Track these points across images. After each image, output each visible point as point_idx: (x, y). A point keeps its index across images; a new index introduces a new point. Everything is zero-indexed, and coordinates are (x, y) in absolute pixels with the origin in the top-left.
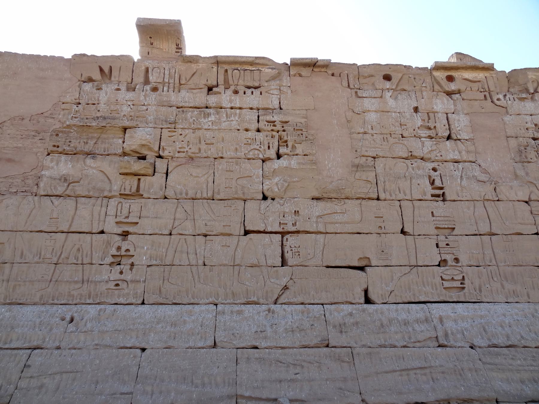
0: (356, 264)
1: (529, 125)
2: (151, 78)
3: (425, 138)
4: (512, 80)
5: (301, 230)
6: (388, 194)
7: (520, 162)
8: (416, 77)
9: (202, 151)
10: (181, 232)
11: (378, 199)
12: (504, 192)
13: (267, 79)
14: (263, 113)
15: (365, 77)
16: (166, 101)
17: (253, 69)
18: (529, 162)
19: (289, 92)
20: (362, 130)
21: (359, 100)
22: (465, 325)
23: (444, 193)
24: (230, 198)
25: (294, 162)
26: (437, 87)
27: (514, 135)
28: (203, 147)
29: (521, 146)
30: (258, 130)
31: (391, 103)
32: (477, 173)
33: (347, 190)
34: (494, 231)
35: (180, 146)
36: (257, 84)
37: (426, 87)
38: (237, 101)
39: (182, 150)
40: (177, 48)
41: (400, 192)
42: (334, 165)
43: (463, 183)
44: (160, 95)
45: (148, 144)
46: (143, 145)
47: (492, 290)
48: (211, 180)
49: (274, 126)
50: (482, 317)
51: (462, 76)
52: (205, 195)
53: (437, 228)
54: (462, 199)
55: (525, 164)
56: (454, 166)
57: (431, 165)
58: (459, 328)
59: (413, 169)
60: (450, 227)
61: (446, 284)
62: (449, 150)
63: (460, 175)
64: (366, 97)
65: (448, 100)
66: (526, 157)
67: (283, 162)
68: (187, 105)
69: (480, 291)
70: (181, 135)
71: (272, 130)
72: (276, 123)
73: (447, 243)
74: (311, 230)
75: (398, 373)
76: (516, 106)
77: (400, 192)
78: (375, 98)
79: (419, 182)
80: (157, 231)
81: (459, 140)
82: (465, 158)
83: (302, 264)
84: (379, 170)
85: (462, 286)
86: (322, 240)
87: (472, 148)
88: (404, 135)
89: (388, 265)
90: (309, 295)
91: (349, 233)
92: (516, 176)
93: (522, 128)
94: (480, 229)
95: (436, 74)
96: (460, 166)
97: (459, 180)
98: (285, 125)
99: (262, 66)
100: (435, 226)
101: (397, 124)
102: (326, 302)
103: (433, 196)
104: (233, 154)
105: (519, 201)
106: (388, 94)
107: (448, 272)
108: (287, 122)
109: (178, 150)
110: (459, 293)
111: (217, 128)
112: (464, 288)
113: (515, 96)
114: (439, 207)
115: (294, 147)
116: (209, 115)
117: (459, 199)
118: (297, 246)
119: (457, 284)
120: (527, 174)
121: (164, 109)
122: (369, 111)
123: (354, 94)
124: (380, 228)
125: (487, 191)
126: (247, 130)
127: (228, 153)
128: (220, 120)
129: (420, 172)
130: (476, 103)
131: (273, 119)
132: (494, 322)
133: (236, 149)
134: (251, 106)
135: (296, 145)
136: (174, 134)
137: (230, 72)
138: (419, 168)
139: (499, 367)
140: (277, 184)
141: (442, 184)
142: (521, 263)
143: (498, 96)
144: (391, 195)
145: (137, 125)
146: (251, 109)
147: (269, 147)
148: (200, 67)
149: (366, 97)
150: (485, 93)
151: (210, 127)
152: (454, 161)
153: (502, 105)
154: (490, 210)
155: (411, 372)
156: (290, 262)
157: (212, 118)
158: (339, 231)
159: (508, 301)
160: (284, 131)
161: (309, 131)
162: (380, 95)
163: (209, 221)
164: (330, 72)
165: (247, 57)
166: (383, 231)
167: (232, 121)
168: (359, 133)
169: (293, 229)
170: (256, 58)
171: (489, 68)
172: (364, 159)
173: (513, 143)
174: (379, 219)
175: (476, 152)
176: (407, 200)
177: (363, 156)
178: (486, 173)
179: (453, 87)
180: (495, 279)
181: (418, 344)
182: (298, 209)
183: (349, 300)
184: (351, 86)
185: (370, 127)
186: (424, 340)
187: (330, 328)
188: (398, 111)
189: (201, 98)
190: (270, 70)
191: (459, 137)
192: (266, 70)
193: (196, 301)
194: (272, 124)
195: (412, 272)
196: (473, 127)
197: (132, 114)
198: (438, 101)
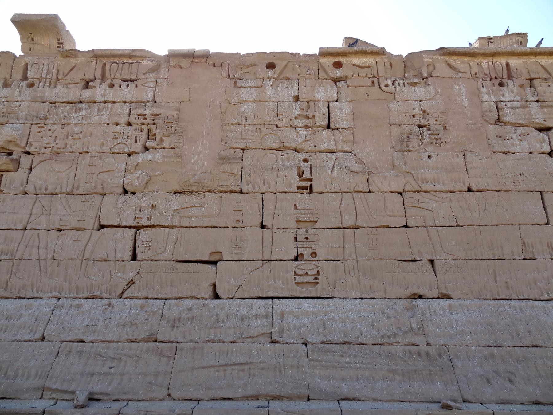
0: (206, 258)
1: (416, 112)
2: (29, 74)
3: (302, 128)
4: (408, 64)
5: (156, 224)
6: (251, 186)
7: (400, 151)
8: (302, 64)
9: (68, 146)
10: (35, 227)
11: (241, 192)
12: (377, 183)
13: (145, 71)
14: (136, 106)
15: (248, 67)
16: (40, 97)
17: (132, 62)
18: (410, 151)
19: (166, 84)
20: (235, 121)
21: (237, 90)
22: (307, 321)
23: (311, 185)
24: (89, 193)
25: (158, 156)
26: (322, 74)
27: (397, 122)
28: (70, 141)
29: (404, 134)
30: (130, 124)
31: (270, 92)
32: (351, 163)
33: (209, 183)
34: (359, 224)
35: (47, 142)
36: (134, 77)
37: (310, 74)
38: (111, 95)
39: (48, 145)
40: (59, 43)
41: (264, 185)
42: (200, 158)
43: (333, 174)
44: (35, 91)
45: (14, 140)
46: (9, 141)
47: (346, 285)
48: (72, 175)
49: (145, 119)
50: (326, 313)
51: (350, 61)
52: (64, 190)
53: (298, 221)
54: (329, 191)
55: (405, 153)
56: (327, 157)
57: (301, 156)
58: (298, 324)
59: (282, 161)
60: (312, 220)
61: (299, 279)
62: (325, 140)
63: (332, 165)
64: (246, 87)
65: (332, 88)
66: (407, 146)
67: (148, 156)
68: (60, 100)
69: (334, 286)
70: (50, 130)
71: (143, 124)
72: (146, 117)
73: (306, 236)
74: (166, 224)
75: (215, 369)
76: (405, 91)
77: (264, 185)
78: (254, 87)
79: (286, 174)
80: (11, 226)
81: (338, 129)
82: (340, 148)
83: (152, 258)
84: (246, 162)
85: (315, 281)
86: (175, 234)
87: (351, 137)
88: (279, 125)
89: (240, 259)
90: (154, 290)
91: (205, 227)
92: (394, 166)
93: (408, 115)
94: (344, 222)
95: (323, 60)
96: (334, 156)
97: (330, 171)
98: (155, 118)
99: (142, 59)
100: (296, 219)
101: (274, 114)
102: (170, 297)
103: (298, 188)
104: (98, 149)
105: (391, 192)
106: (268, 83)
107: (302, 266)
108: (158, 115)
109: (45, 145)
110: (310, 289)
111: (86, 122)
112: (318, 283)
113: (406, 81)
114: (305, 200)
115: (162, 140)
116: (80, 109)
117: (326, 191)
118: (149, 240)
119: (311, 279)
120: (406, 163)
121: (37, 104)
122: (246, 101)
123: (232, 84)
124: (238, 222)
125: (360, 182)
126: (117, 124)
127: (94, 148)
128: (91, 114)
129: (288, 164)
130: (362, 90)
131: (145, 113)
132: (337, 318)
133: (103, 143)
134: (124, 100)
135: (164, 138)
136: (43, 129)
137: (108, 66)
138: (288, 159)
139: (324, 364)
140: (138, 178)
141: (311, 176)
142: (384, 258)
143: (386, 82)
144: (254, 188)
145: (8, 121)
146: (125, 102)
147: (136, 141)
148: (79, 61)
149: (246, 87)
150: (374, 79)
151: (80, 122)
152: (329, 151)
153: (390, 91)
154: (358, 202)
155: (229, 368)
156: (139, 257)
157: (83, 113)
158: (194, 225)
159: (363, 297)
160: (154, 124)
161: (180, 124)
162: (259, 84)
163: (65, 215)
164: (211, 62)
165: (123, 50)
166: (241, 224)
167: (103, 115)
168: (232, 125)
169: (148, 223)
170: (133, 50)
171: (381, 52)
172: (232, 151)
173: (396, 131)
174: (238, 212)
175: (354, 142)
176: (271, 193)
177: (232, 148)
178: (361, 164)
179: (339, 73)
180: (352, 274)
181: (249, 340)
182: (155, 203)
183: (193, 295)
184: (231, 76)
185: (244, 118)
186: (257, 336)
187: (163, 323)
188: (277, 101)
189: (76, 92)
190: (149, 62)
191: (337, 126)
192: (145, 63)
193: (39, 295)
194: (143, 117)
195: (264, 266)
196: (355, 116)
197: (4, 111)
198: (321, 88)
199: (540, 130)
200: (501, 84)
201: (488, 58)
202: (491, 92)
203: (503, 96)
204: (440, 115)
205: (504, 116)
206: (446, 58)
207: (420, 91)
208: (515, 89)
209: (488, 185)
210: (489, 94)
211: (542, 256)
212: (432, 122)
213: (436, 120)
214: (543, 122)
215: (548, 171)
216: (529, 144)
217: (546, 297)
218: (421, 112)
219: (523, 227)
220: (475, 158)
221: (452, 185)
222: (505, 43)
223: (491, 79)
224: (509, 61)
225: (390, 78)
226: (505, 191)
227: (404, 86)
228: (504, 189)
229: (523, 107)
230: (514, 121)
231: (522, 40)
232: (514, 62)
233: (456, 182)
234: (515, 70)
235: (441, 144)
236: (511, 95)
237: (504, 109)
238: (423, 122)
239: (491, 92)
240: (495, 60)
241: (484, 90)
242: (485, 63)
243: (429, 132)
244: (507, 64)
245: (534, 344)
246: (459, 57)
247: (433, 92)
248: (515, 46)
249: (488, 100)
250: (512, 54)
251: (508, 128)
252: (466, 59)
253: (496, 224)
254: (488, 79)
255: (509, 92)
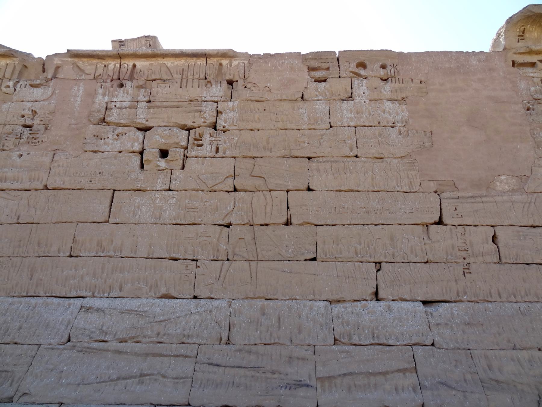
66: (3, 146)
93: (16, 115)
113: (29, 82)
143: (8, 84)
153: (8, 92)
199: (139, 129)
200: (122, 86)
201: (116, 60)
202: (107, 93)
203: (117, 96)
204: (47, 115)
205: (109, 116)
206: (76, 60)
207: (37, 93)
208: (130, 91)
209: (64, 183)
210: (104, 95)
211: (87, 254)
212: (36, 122)
213: (41, 120)
214: (144, 122)
215: (128, 169)
216: (121, 143)
217: (74, 294)
218: (30, 112)
219: (80, 225)
220: (63, 157)
221: (29, 183)
222: (135, 46)
223: (112, 81)
224: (136, 63)
225: (13, 80)
226: (79, 189)
227: (25, 87)
228: (78, 187)
229: (130, 107)
230: (116, 121)
231: (151, 43)
232: (141, 64)
233: (34, 180)
234: (138, 72)
235: (37, 144)
236: (126, 95)
237: (112, 109)
238: (29, 122)
239: (107, 93)
240: (123, 62)
241: (101, 91)
242: (113, 65)
243: (30, 132)
244: (134, 66)
245: (15, 341)
246: (88, 59)
247: (49, 93)
248: (144, 48)
249: (101, 99)
250: (135, 56)
251: (108, 127)
252: (95, 61)
253: (56, 221)
254: (109, 80)
255: (124, 93)
